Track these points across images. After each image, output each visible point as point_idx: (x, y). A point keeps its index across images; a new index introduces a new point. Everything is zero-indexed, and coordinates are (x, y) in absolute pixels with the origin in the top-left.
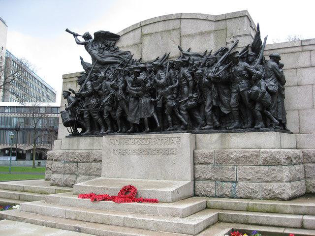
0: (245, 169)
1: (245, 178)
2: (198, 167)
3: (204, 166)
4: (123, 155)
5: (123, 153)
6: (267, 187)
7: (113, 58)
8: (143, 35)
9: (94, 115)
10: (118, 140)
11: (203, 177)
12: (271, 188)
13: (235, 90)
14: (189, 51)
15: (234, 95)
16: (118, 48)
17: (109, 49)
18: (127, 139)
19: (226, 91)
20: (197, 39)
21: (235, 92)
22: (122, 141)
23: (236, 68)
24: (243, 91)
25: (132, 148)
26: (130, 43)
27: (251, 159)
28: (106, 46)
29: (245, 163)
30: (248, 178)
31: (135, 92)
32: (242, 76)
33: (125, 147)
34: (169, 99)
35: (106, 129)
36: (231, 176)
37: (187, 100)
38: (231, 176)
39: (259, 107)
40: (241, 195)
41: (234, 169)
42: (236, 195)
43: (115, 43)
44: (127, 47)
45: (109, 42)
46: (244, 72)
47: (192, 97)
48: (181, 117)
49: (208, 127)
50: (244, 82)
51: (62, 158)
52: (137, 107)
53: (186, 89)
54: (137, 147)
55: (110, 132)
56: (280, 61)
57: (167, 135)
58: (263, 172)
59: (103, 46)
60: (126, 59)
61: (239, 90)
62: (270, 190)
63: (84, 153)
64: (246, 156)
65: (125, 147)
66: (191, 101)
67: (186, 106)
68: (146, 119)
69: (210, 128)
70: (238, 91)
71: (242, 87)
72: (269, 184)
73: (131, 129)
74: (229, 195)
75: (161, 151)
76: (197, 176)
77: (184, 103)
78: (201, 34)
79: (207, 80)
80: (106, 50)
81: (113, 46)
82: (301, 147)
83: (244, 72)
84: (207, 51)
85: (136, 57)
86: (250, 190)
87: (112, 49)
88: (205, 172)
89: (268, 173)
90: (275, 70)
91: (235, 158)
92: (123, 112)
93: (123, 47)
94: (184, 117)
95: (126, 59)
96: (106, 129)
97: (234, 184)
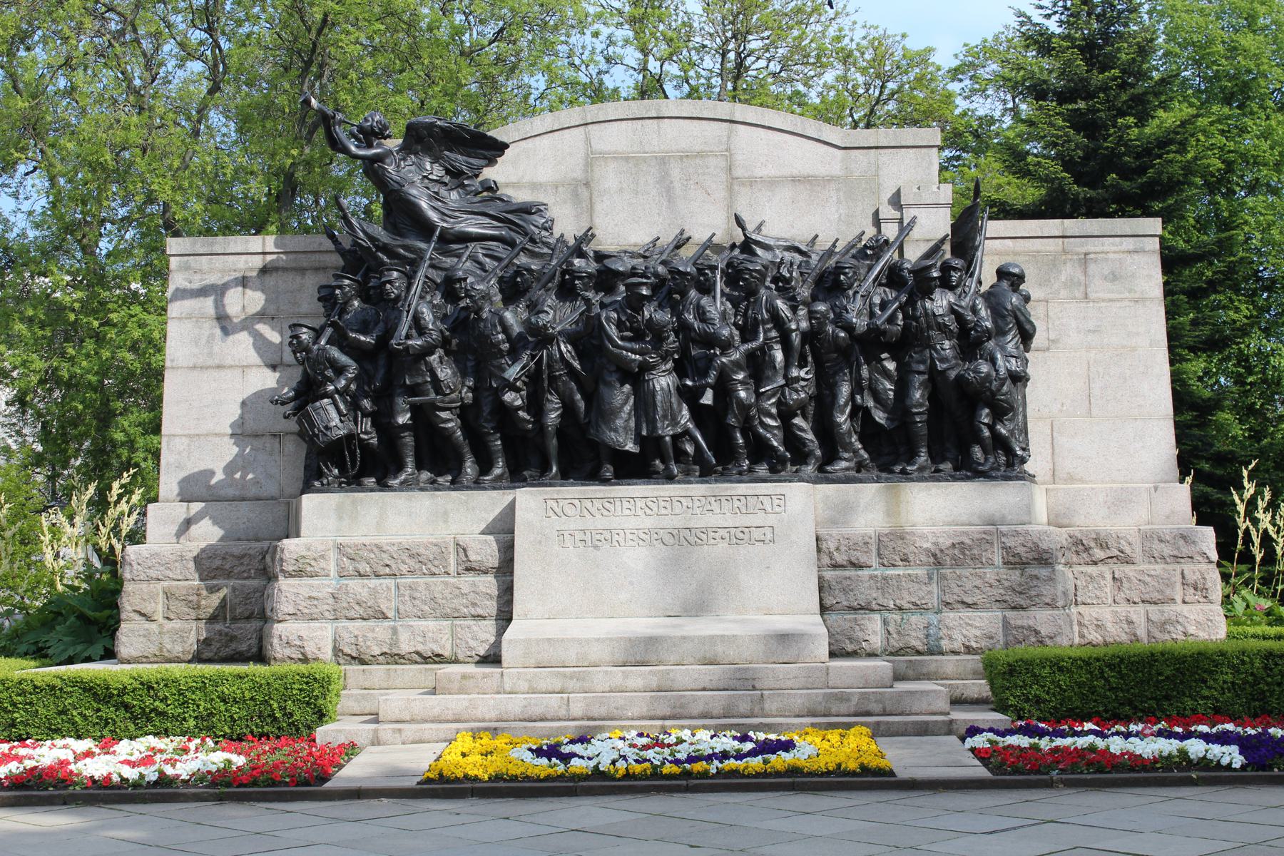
0: (959, 577)
1: (963, 602)
2: (829, 574)
3: (847, 573)
4: (596, 547)
5: (593, 541)
6: (1019, 623)
7: (489, 221)
8: (592, 160)
9: (444, 415)
10: (576, 502)
11: (845, 603)
12: (1031, 623)
13: (922, 368)
14: (759, 228)
15: (918, 379)
16: (490, 188)
17: (462, 186)
18: (611, 500)
19: (891, 366)
20: (786, 192)
21: (920, 373)
22: (588, 504)
23: (928, 304)
24: (944, 371)
26: (545, 174)
27: (976, 552)
28: (448, 172)
29: (957, 563)
30: (969, 600)
31: (633, 356)
32: (943, 328)
33: (600, 522)
34: (742, 382)
35: (485, 466)
36: (923, 598)
37: (782, 387)
38: (923, 598)
39: (987, 415)
40: (957, 646)
41: (930, 578)
42: (939, 647)
43: (481, 168)
44: (534, 186)
45: (460, 160)
46: (949, 320)
47: (798, 379)
48: (768, 435)
49: (844, 464)
50: (947, 344)
51: (323, 564)
53: (779, 356)
54: (648, 523)
55: (499, 478)
56: (1021, 287)
57: (742, 488)
58: (1007, 584)
59: (437, 172)
60: (537, 231)
61: (933, 365)
62: (1029, 628)
63: (426, 547)
64: (962, 543)
65: (600, 522)
66: (797, 391)
67: (779, 404)
69: (847, 469)
70: (932, 369)
71: (943, 360)
72: (1022, 613)
73: (410, 465)
74: (920, 648)
75: (723, 533)
76: (829, 601)
77: (773, 396)
78: (796, 180)
79: (842, 334)
80: (446, 184)
81: (477, 176)
82: (1065, 521)
83: (949, 320)
84: (817, 236)
85: (566, 225)
86: (978, 633)
87: (475, 184)
88: (852, 590)
89: (1020, 585)
90: (1018, 313)
91: (933, 548)
92: (568, 409)
93: (516, 185)
94: (774, 435)
95: (537, 231)
96: (485, 466)
97: (934, 618)
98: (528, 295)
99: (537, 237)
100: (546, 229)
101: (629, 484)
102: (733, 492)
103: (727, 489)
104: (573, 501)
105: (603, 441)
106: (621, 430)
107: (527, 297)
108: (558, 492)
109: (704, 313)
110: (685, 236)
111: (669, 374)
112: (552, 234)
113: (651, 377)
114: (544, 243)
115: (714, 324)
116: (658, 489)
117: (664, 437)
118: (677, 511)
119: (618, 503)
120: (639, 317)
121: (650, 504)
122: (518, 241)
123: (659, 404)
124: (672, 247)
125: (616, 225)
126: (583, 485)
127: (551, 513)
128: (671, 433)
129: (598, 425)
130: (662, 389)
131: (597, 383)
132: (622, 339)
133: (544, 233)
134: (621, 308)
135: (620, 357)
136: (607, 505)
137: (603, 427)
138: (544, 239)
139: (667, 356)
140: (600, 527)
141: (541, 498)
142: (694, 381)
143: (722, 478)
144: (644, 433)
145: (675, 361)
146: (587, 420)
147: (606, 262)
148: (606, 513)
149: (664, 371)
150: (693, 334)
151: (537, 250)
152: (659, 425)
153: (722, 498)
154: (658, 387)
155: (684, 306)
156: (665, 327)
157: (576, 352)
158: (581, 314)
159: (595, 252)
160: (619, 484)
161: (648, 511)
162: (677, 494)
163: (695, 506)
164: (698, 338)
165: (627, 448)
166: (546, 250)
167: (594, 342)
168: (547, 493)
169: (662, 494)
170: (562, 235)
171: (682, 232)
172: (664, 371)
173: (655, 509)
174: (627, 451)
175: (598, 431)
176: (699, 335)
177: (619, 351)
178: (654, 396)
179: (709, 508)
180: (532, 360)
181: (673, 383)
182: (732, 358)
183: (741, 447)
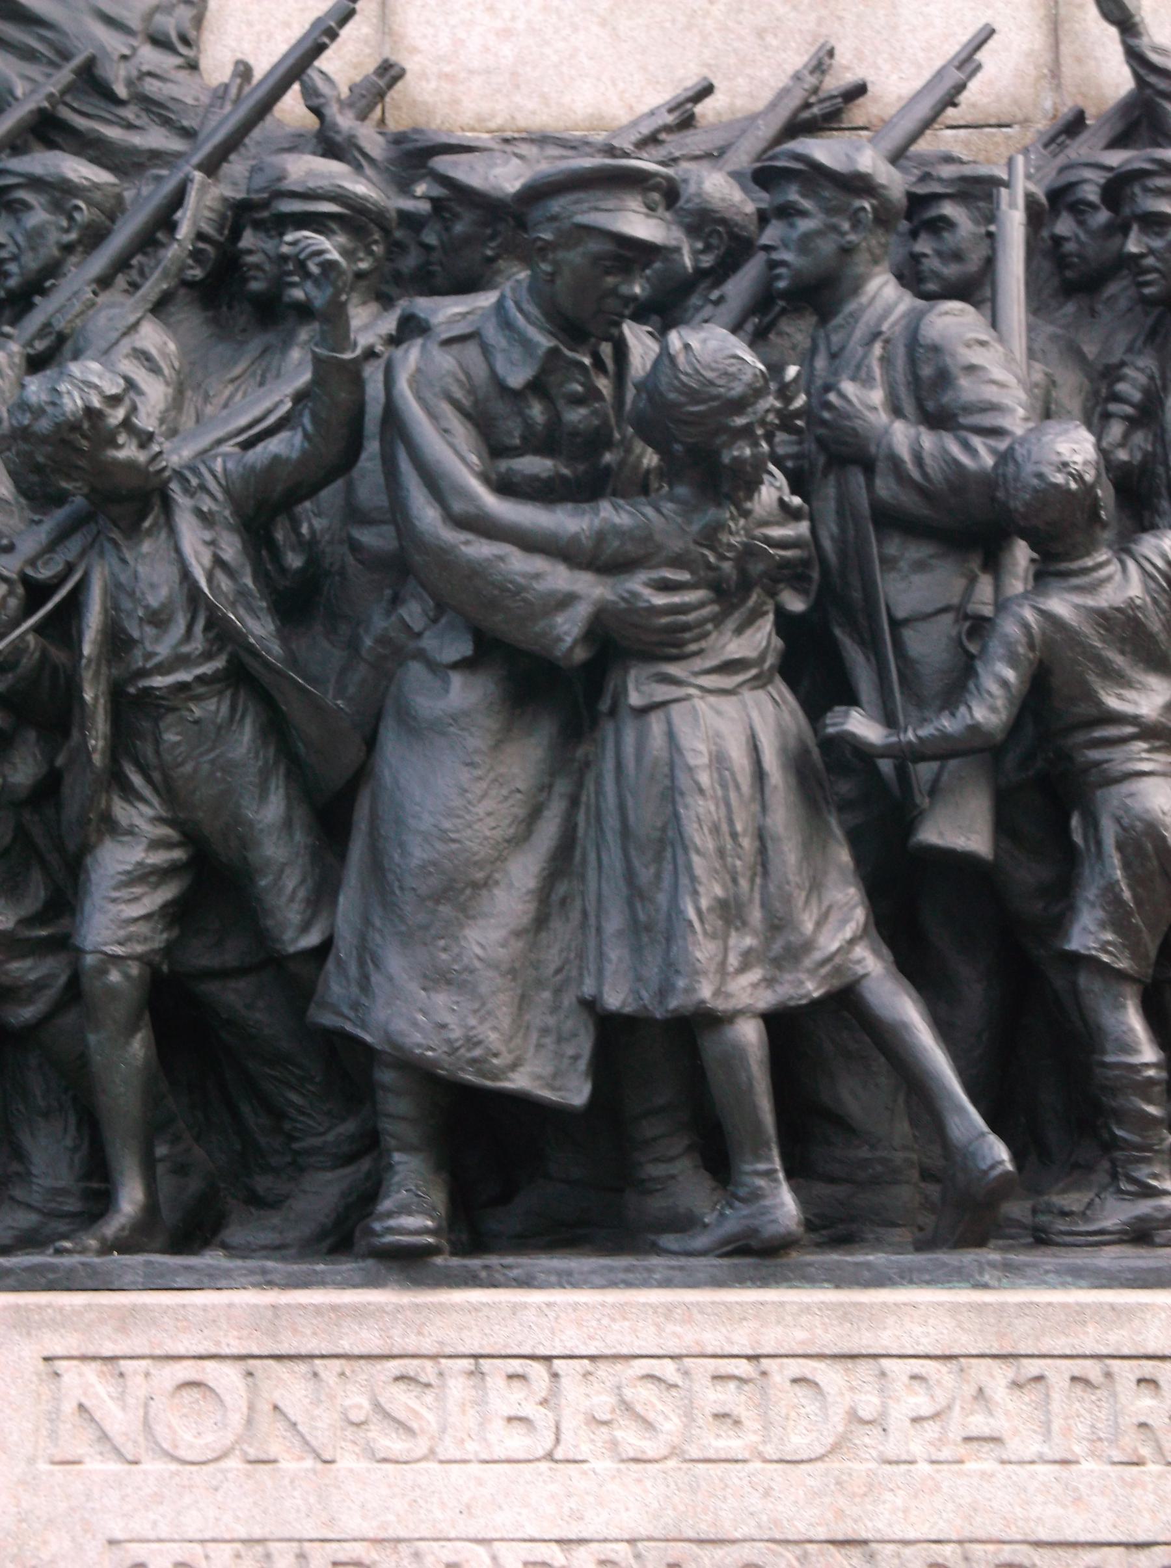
10: (225, 1377)
25: (502, 1522)
52: (548, 831)
60: (114, 43)
68: (750, 1033)
95: (114, 43)
98: (44, 310)
99: (119, 82)
100: (160, 42)
101: (526, 1282)
102: (1118, 1339)
103: (1080, 1313)
104: (211, 1371)
105: (388, 1037)
106: (488, 980)
107: (34, 321)
108: (125, 1321)
109: (943, 378)
110: (834, 83)
111: (760, 682)
112: (193, 66)
113: (662, 692)
114: (149, 104)
115: (996, 432)
116: (688, 1313)
117: (728, 1018)
118: (799, 1441)
119: (458, 1388)
120: (604, 384)
121: (644, 1396)
122: (20, 89)
123: (701, 838)
124: (767, 129)
125: (506, 33)
126: (268, 1283)
127: (80, 1444)
128: (766, 1000)
129: (368, 956)
130: (719, 761)
131: (371, 742)
132: (505, 487)
133: (150, 57)
134: (507, 325)
135: (475, 572)
136: (401, 1399)
137: (396, 962)
138: (151, 87)
139: (745, 585)
140: (353, 1524)
141: (28, 1352)
142: (890, 721)
143: (1046, 1259)
144: (615, 999)
145: (785, 623)
146: (312, 939)
147: (443, 164)
148: (395, 1444)
149: (729, 667)
150: (885, 487)
151: (113, 133)
152: (704, 951)
153: (1058, 1373)
154: (696, 750)
155: (833, 356)
156: (739, 405)
157: (260, 574)
158: (300, 397)
159: (398, 139)
160: (471, 1280)
161: (631, 1438)
162: (796, 1337)
163: (899, 1414)
164: (908, 501)
165: (520, 1081)
166: (155, 138)
167: (367, 537)
168: (63, 1321)
169: (713, 1341)
170: (244, 71)
171: (823, 61)
172: (729, 667)
173: (671, 1426)
174: (521, 1102)
175: (365, 984)
176: (924, 492)
177: (480, 549)
178: (671, 794)
179: (979, 1423)
180: (29, 608)
181: (782, 732)
182: (1108, 598)
183: (1145, 1088)
